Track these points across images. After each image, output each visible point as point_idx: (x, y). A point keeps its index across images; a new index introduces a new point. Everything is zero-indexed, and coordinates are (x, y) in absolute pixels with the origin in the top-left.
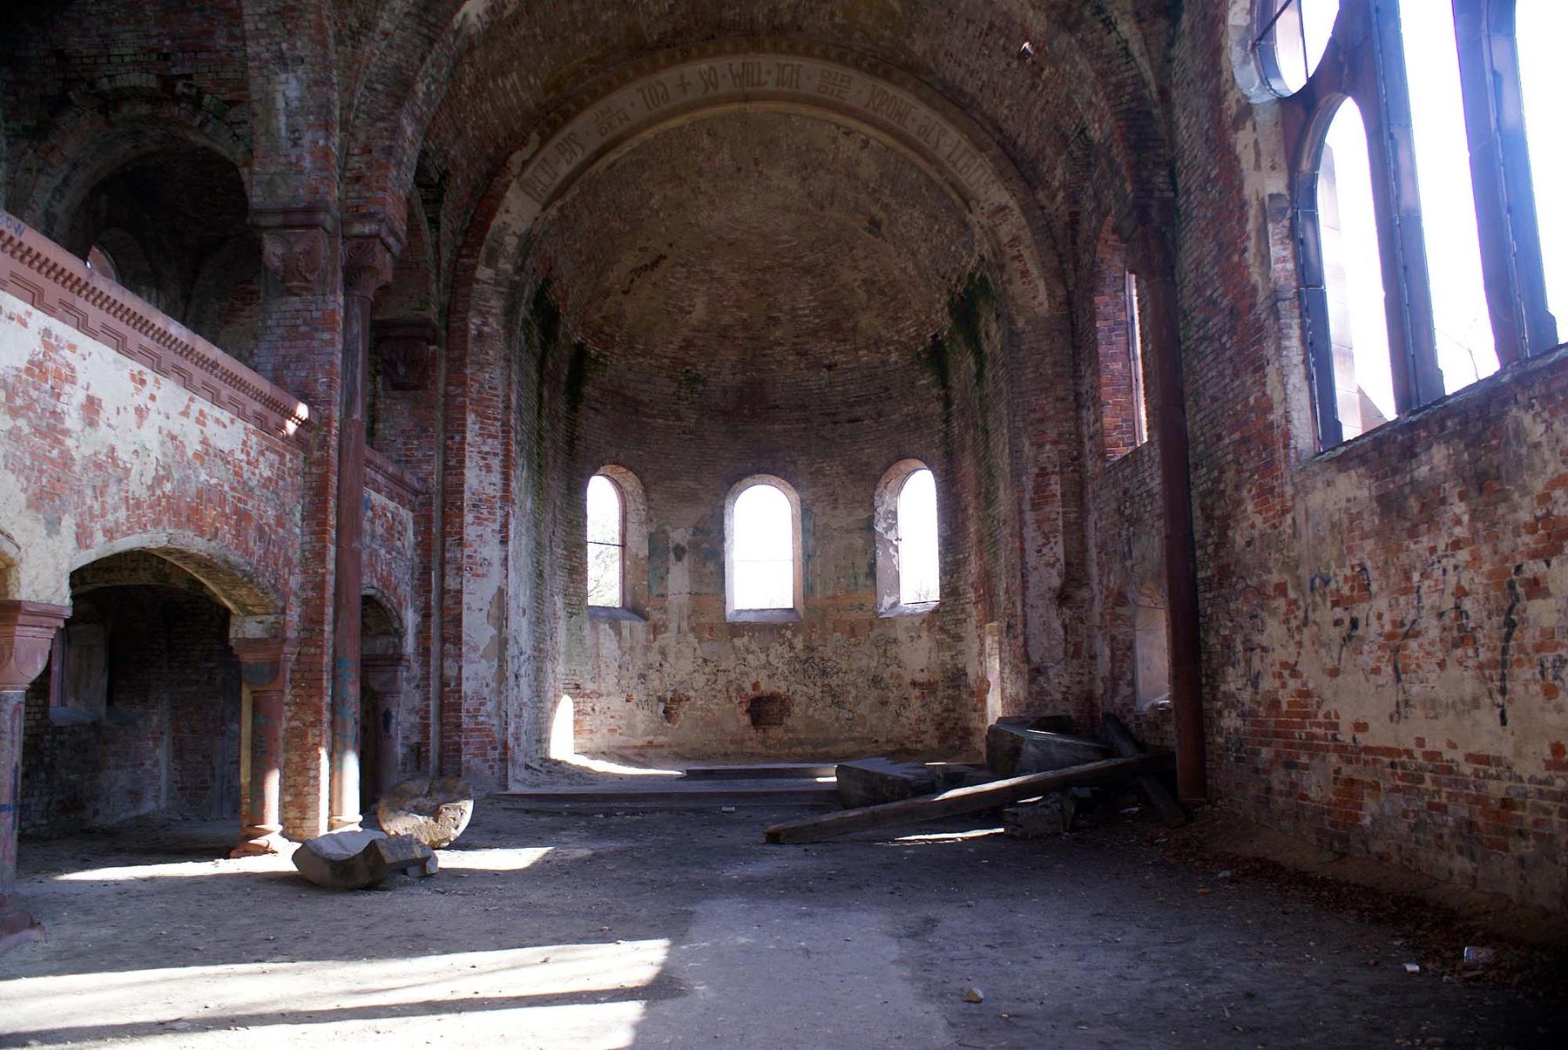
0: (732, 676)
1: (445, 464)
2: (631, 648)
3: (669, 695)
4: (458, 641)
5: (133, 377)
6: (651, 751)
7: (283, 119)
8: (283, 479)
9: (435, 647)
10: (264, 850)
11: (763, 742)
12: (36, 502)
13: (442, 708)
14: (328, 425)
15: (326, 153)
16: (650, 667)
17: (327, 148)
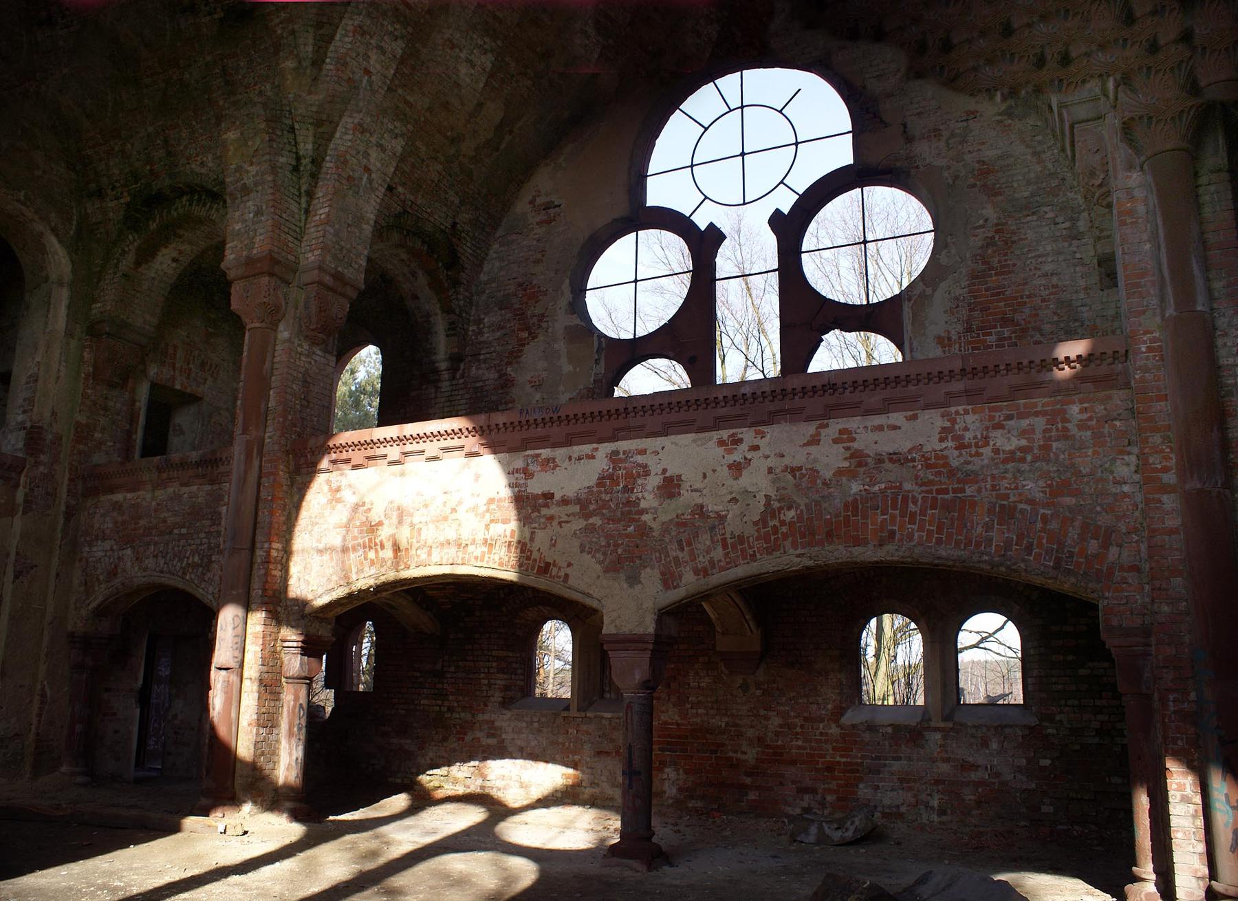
5: (721, 443)
12: (613, 568)
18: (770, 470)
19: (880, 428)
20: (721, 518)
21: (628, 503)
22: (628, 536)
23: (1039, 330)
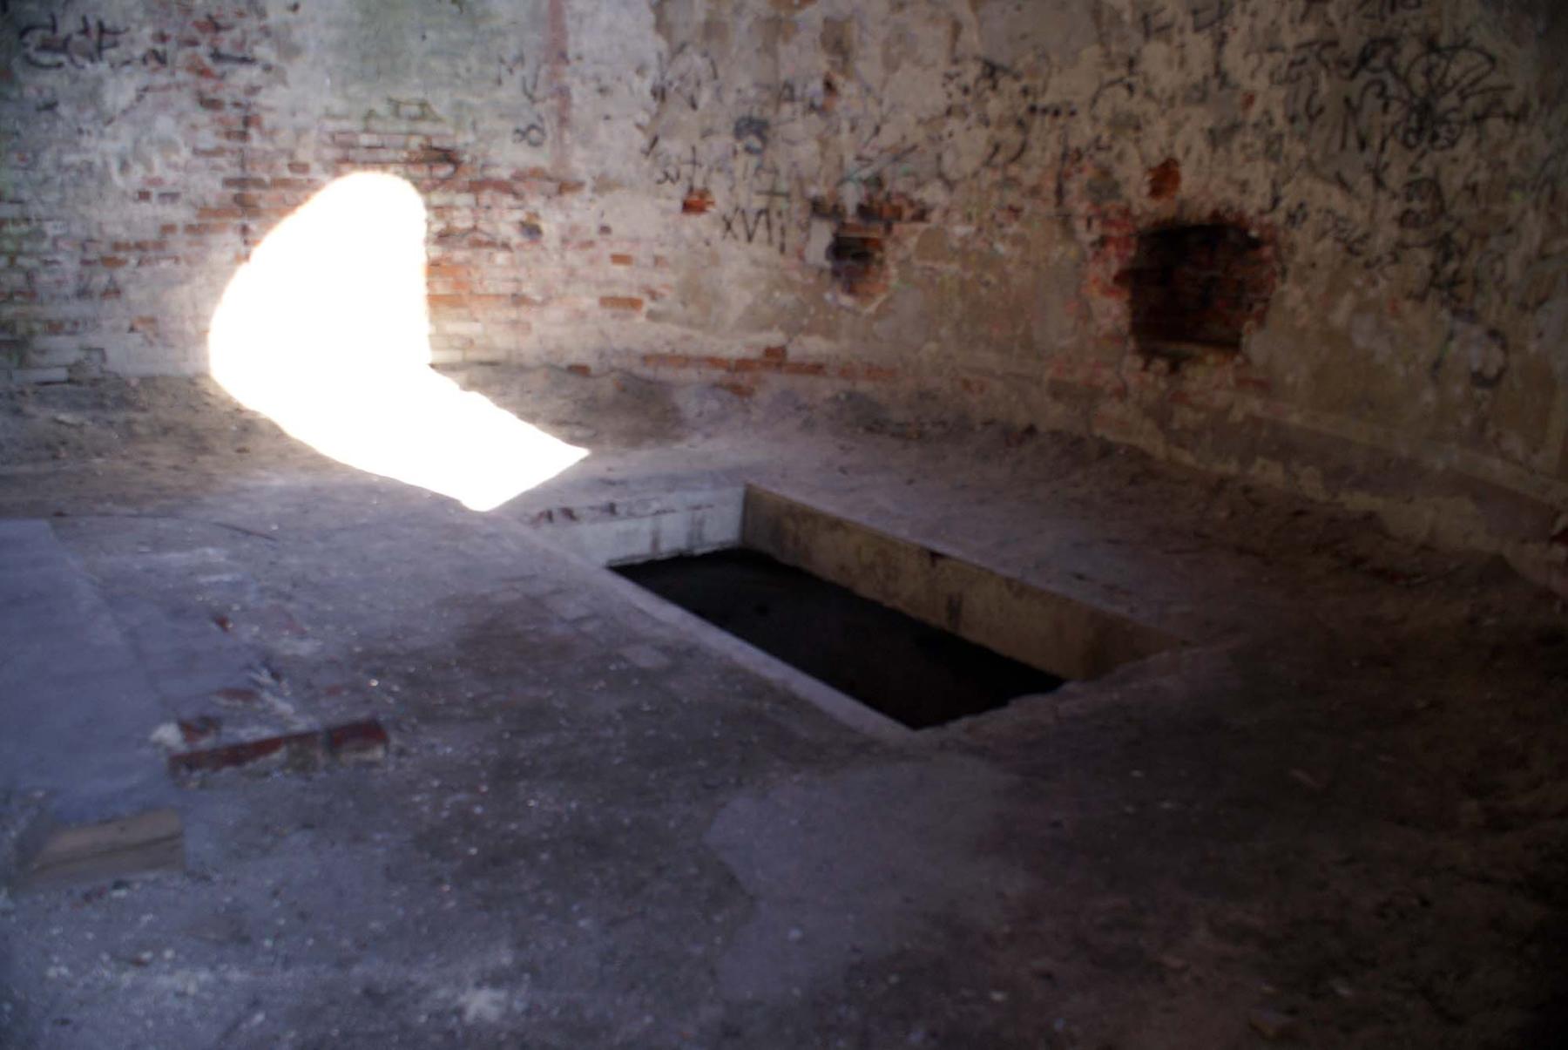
0: (1083, 132)
2: (713, 29)
3: (852, 197)
6: (777, 381)
11: (1160, 416)
16: (786, 93)
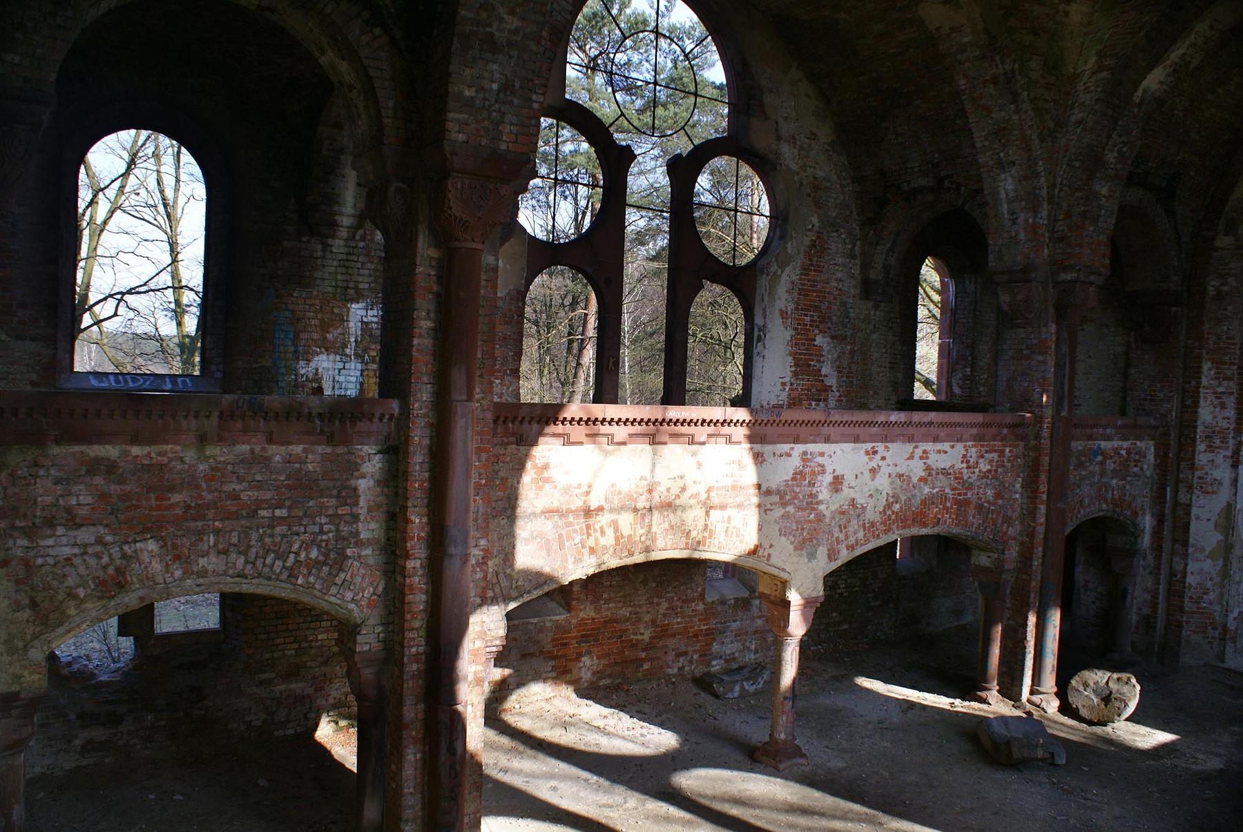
1: (1182, 402)
4: (1185, 543)
5: (867, 453)
7: (1005, 206)
8: (1003, 466)
9: (1167, 546)
10: (984, 701)
12: (799, 548)
13: (1170, 592)
14: (1041, 422)
15: (1035, 227)
17: (1035, 227)
18: (890, 475)
19: (939, 452)
20: (864, 508)
21: (811, 495)
22: (810, 522)
23: (830, 318)
